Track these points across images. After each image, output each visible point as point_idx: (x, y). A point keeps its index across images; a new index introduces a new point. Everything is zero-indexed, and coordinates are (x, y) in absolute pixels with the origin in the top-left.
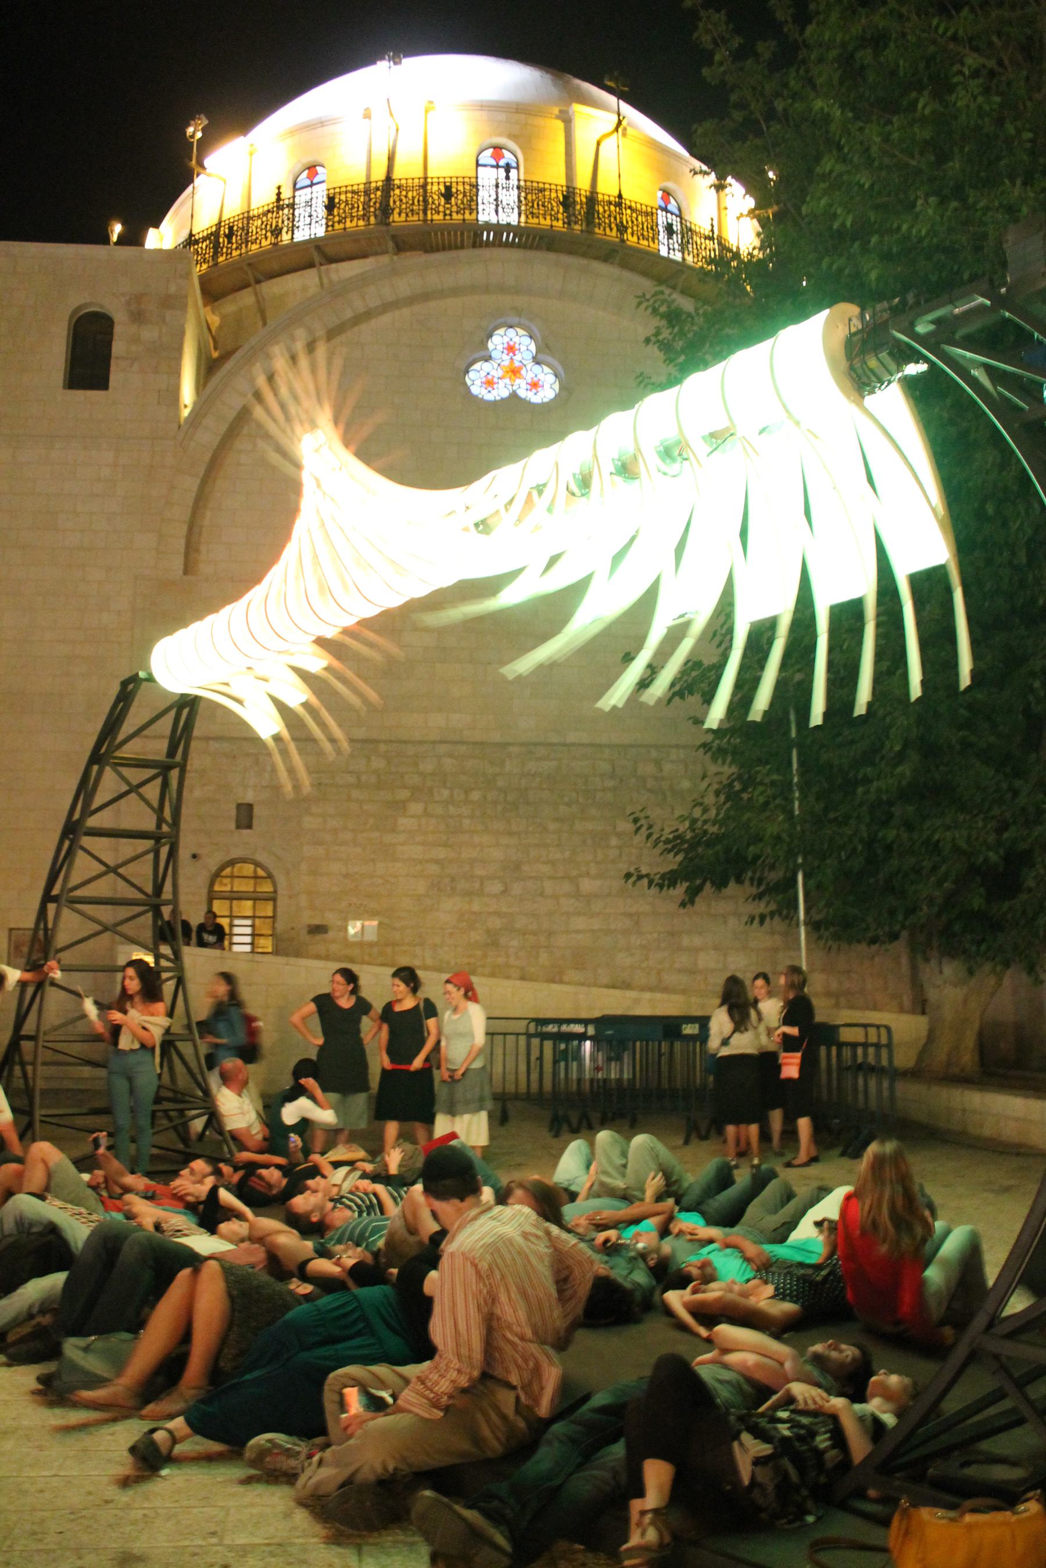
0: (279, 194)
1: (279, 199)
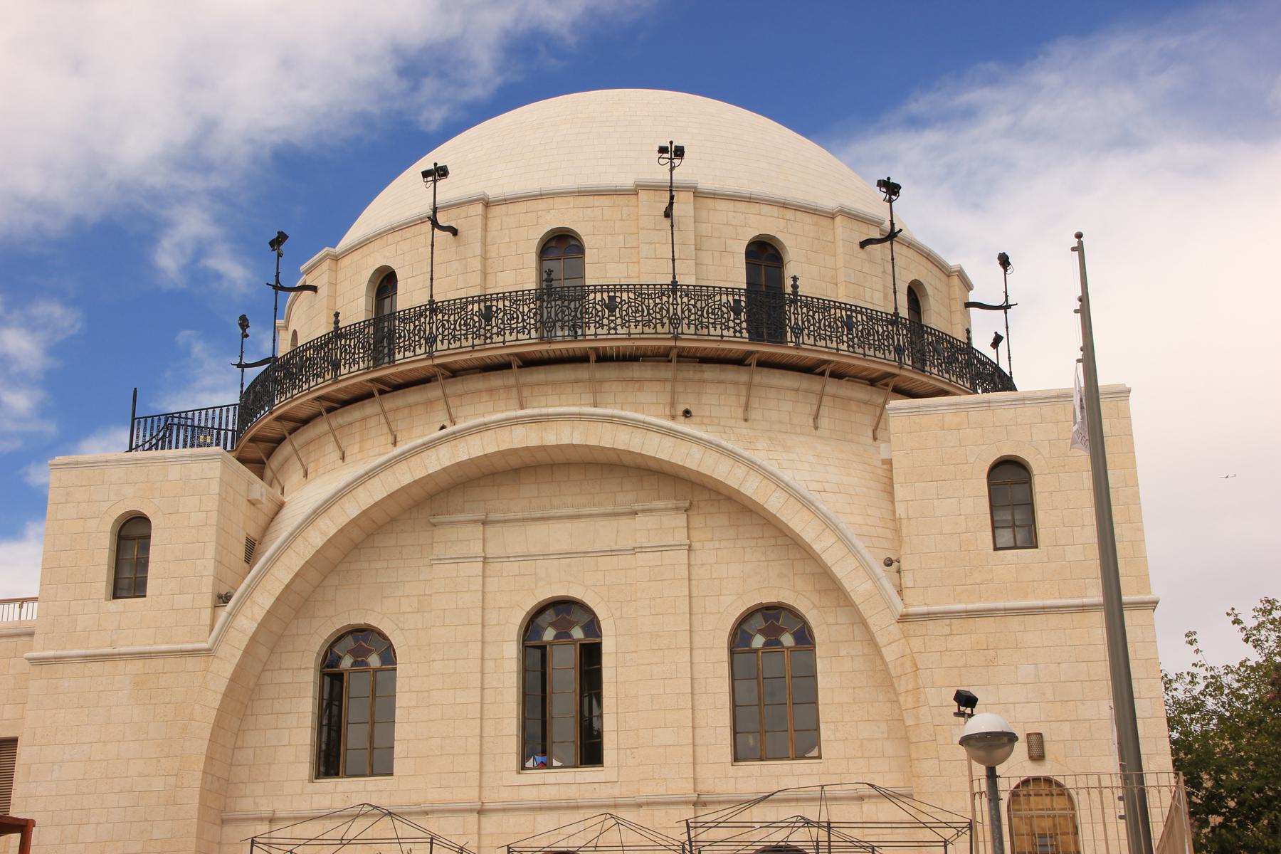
0: (337, 322)
1: (337, 328)
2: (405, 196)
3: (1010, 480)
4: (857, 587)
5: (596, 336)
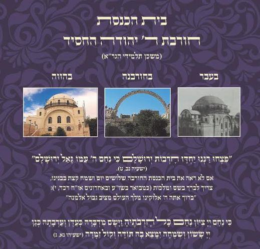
2: (52, 98)
3: (79, 111)
4: (72, 115)
5: (61, 104)
